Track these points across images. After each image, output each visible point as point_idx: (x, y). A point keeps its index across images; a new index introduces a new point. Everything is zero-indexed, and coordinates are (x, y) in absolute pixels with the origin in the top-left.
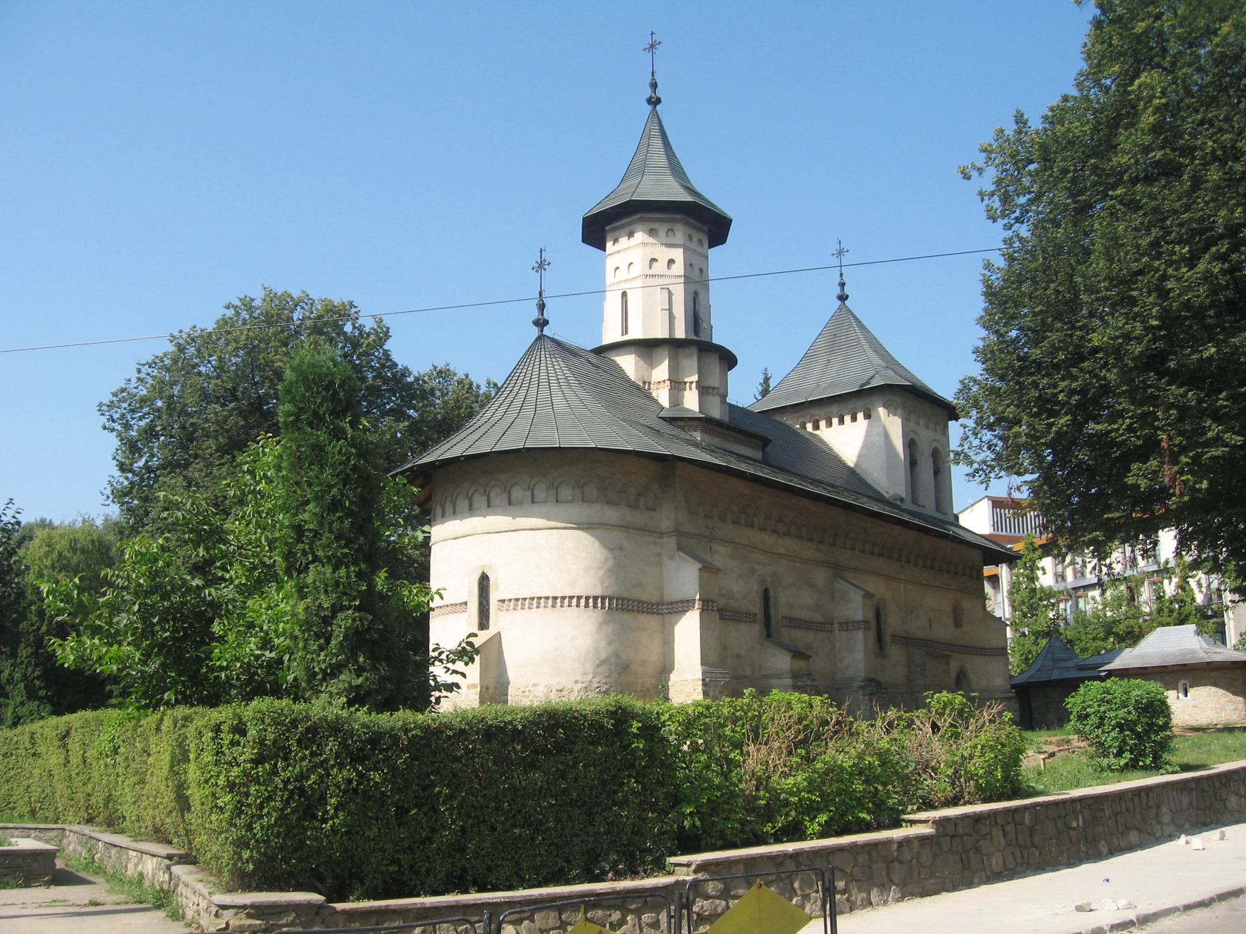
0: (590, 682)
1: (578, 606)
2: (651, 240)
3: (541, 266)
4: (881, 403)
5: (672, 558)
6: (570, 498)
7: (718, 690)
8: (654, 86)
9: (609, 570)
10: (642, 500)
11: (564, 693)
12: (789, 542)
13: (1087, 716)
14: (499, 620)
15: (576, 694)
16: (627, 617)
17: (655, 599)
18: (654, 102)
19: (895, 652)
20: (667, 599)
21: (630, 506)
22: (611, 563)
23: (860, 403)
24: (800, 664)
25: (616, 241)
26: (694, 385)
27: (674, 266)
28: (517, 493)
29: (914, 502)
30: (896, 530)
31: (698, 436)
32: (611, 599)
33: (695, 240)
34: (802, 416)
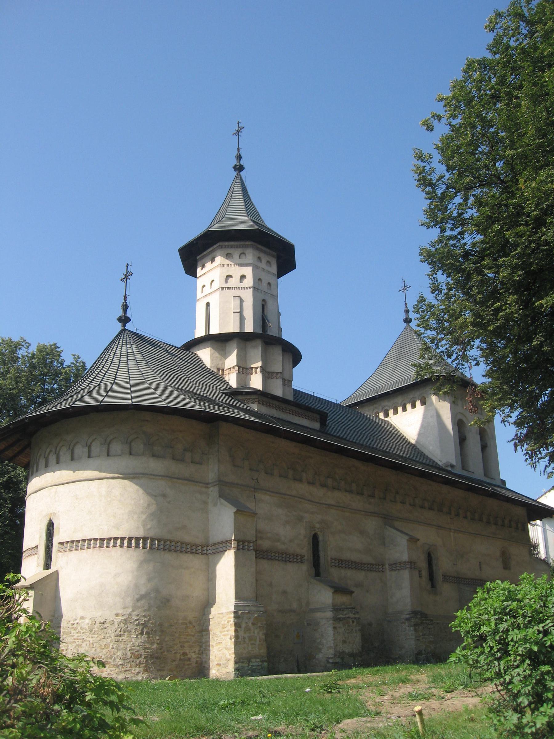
0: (130, 615)
1: (121, 546)
2: (227, 262)
3: (127, 277)
4: (432, 392)
5: (215, 505)
7: (251, 621)
8: (239, 157)
9: (152, 514)
10: (188, 455)
11: (105, 626)
12: (337, 494)
13: (482, 639)
15: (116, 626)
16: (168, 557)
17: (198, 541)
18: (239, 168)
20: (211, 541)
21: (174, 458)
22: (153, 508)
23: (417, 393)
24: (343, 599)
25: (203, 266)
26: (259, 369)
27: (245, 281)
28: (79, 450)
29: (464, 467)
30: (445, 489)
31: (255, 407)
32: (152, 540)
33: (264, 261)
34: (376, 408)
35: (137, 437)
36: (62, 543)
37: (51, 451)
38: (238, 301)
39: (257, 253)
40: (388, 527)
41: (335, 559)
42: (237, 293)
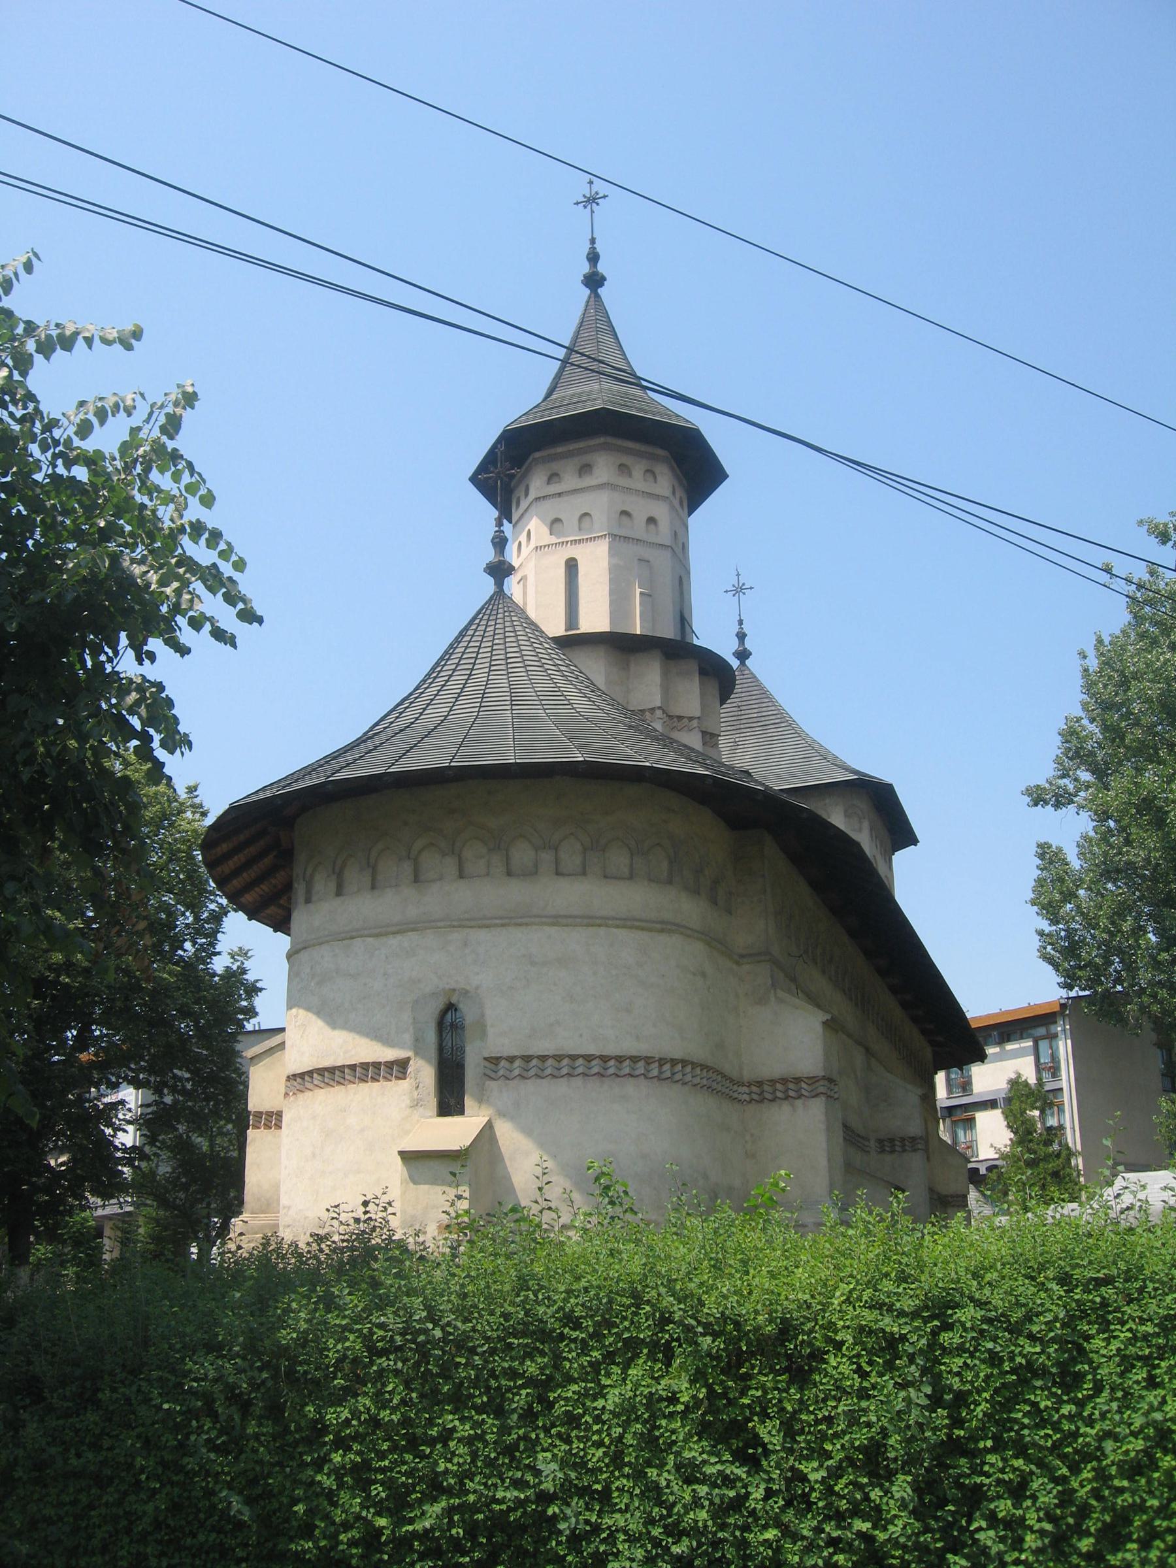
5: (762, 1001)
6: (626, 871)
8: (593, 258)
18: (594, 281)
25: (553, 477)
33: (678, 496)
36: (494, 1061)
42: (647, 553)
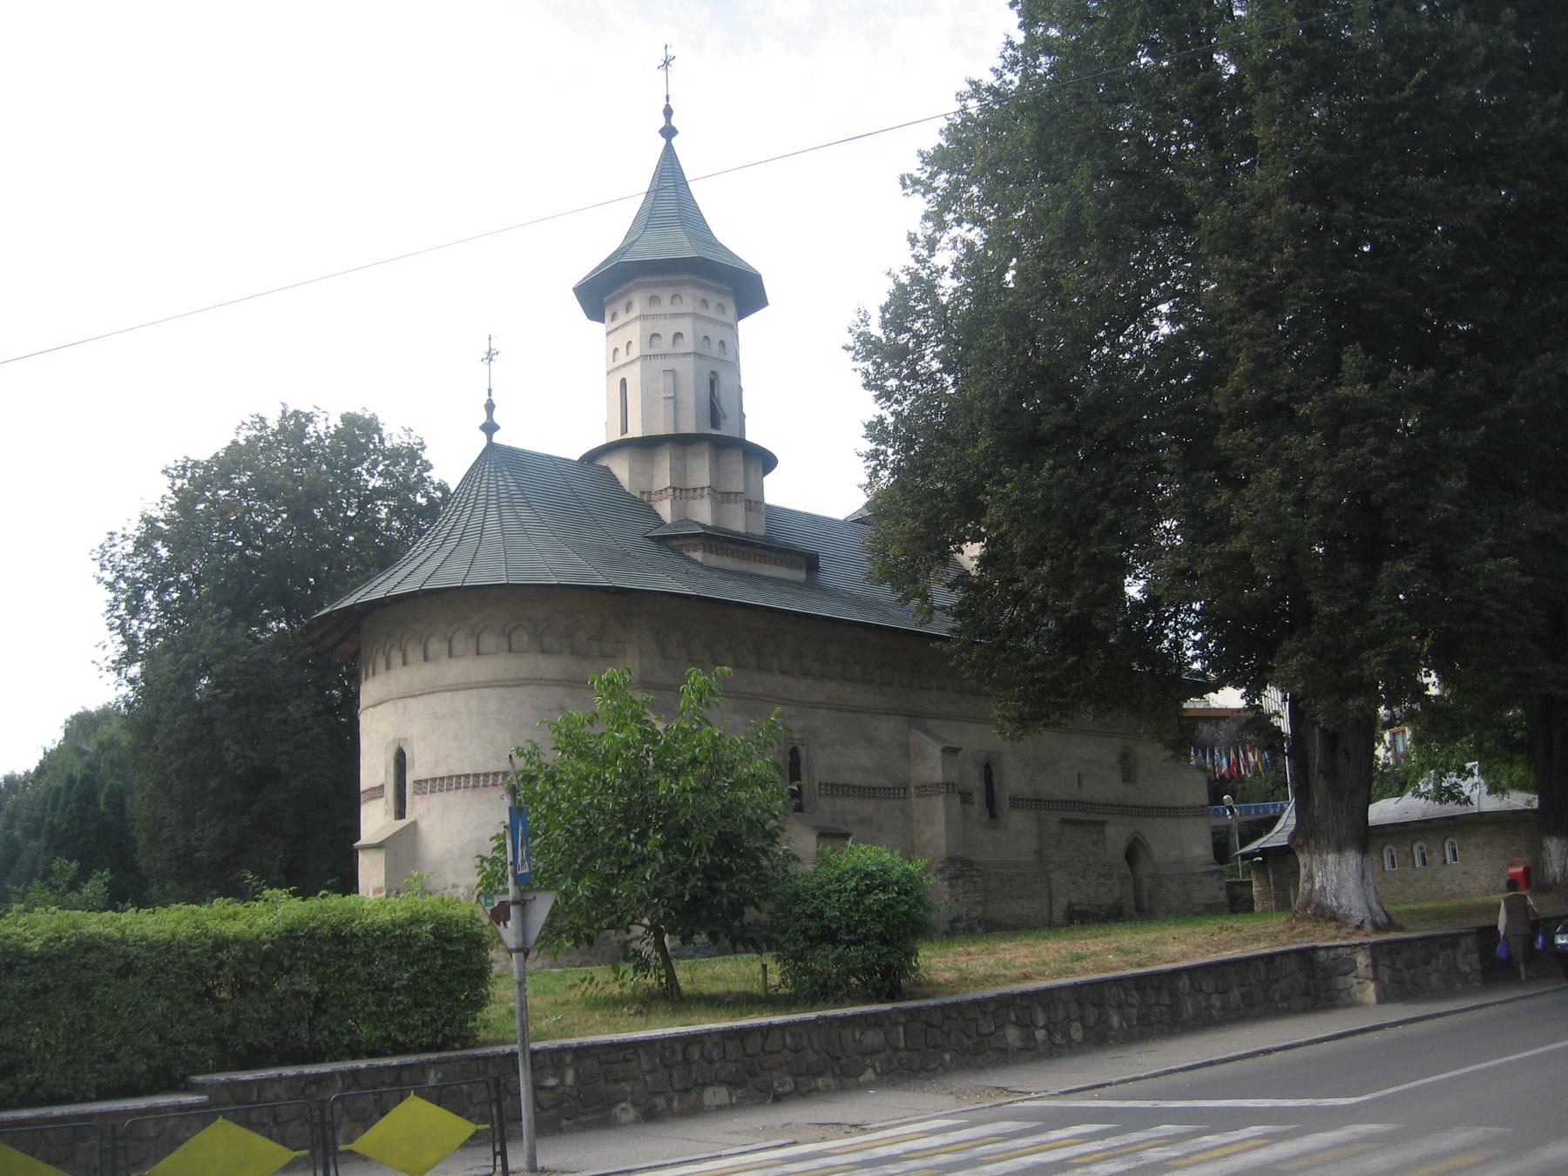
3: (490, 356)
14: (417, 807)
19: (1018, 821)
26: (706, 491)
28: (436, 646)
33: (712, 305)
35: (519, 626)
36: (418, 782)
37: (393, 645)
38: (670, 379)
39: (699, 293)
40: (914, 730)
41: (826, 785)
42: (669, 364)
